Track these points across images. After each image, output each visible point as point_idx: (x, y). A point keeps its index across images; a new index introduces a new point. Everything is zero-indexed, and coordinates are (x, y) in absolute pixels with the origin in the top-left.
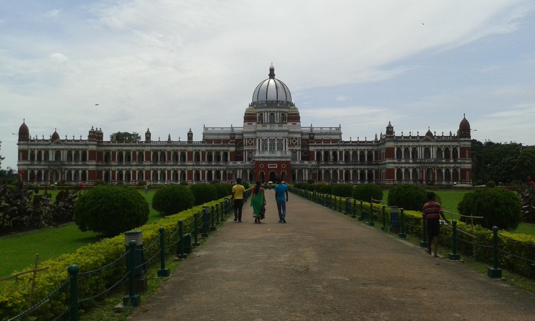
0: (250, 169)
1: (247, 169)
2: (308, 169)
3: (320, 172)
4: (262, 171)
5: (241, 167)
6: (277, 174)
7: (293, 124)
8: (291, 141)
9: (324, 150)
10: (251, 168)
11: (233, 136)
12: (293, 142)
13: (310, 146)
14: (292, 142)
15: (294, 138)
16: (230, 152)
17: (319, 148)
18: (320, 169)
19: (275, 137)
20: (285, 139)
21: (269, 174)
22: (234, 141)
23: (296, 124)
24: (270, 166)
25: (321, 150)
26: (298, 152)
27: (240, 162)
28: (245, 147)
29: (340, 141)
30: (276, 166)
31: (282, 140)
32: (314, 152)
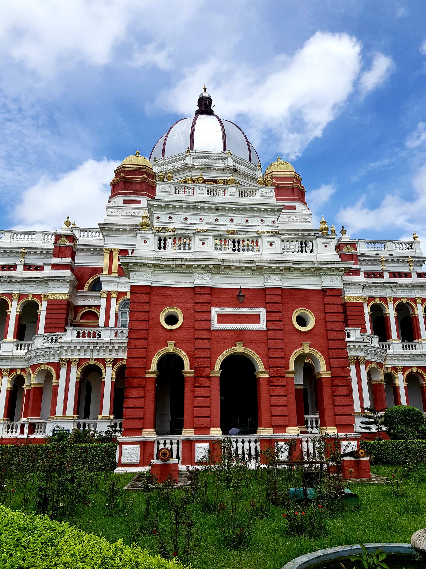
0: (116, 360)
1: (102, 361)
4: (171, 349)
5: (76, 356)
6: (268, 367)
9: (395, 300)
10: (123, 359)
11: (63, 244)
16: (50, 303)
17: (377, 293)
21: (217, 367)
22: (67, 261)
24: (218, 322)
25: (385, 300)
27: (75, 333)
28: (109, 282)
30: (258, 321)
32: (361, 305)
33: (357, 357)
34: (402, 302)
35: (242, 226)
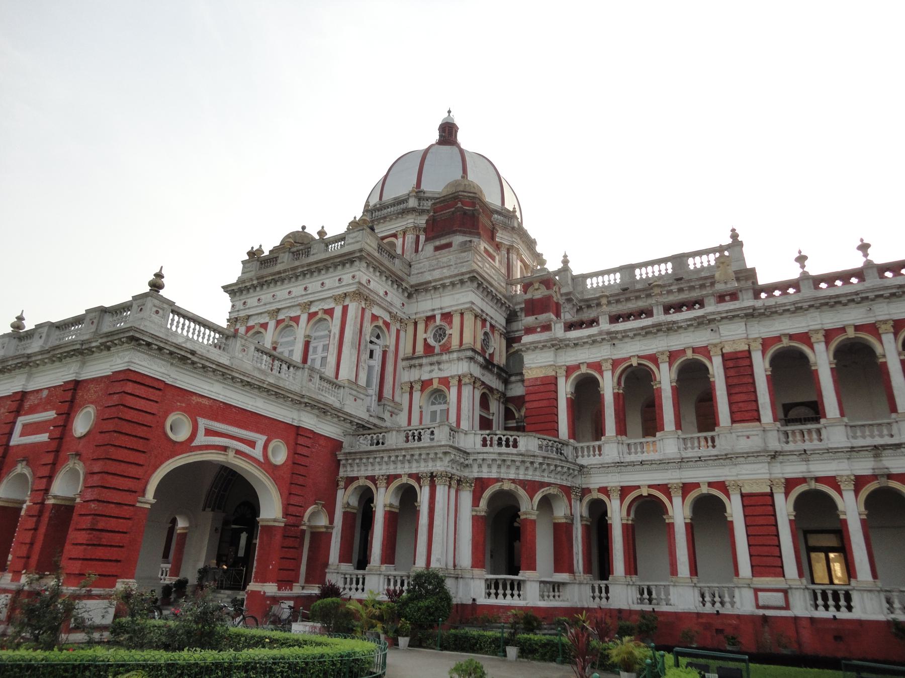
2: (481, 485)
3: (598, 511)
7: (437, 249)
8: (421, 335)
9: (615, 363)
12: (431, 341)
13: (535, 347)
14: (425, 340)
15: (438, 318)
18: (596, 495)
19: (299, 305)
20: (345, 309)
23: (449, 245)
25: (597, 366)
26: (454, 391)
29: (720, 287)
31: (330, 312)
33: (432, 473)
34: (631, 365)
35: (318, 292)
